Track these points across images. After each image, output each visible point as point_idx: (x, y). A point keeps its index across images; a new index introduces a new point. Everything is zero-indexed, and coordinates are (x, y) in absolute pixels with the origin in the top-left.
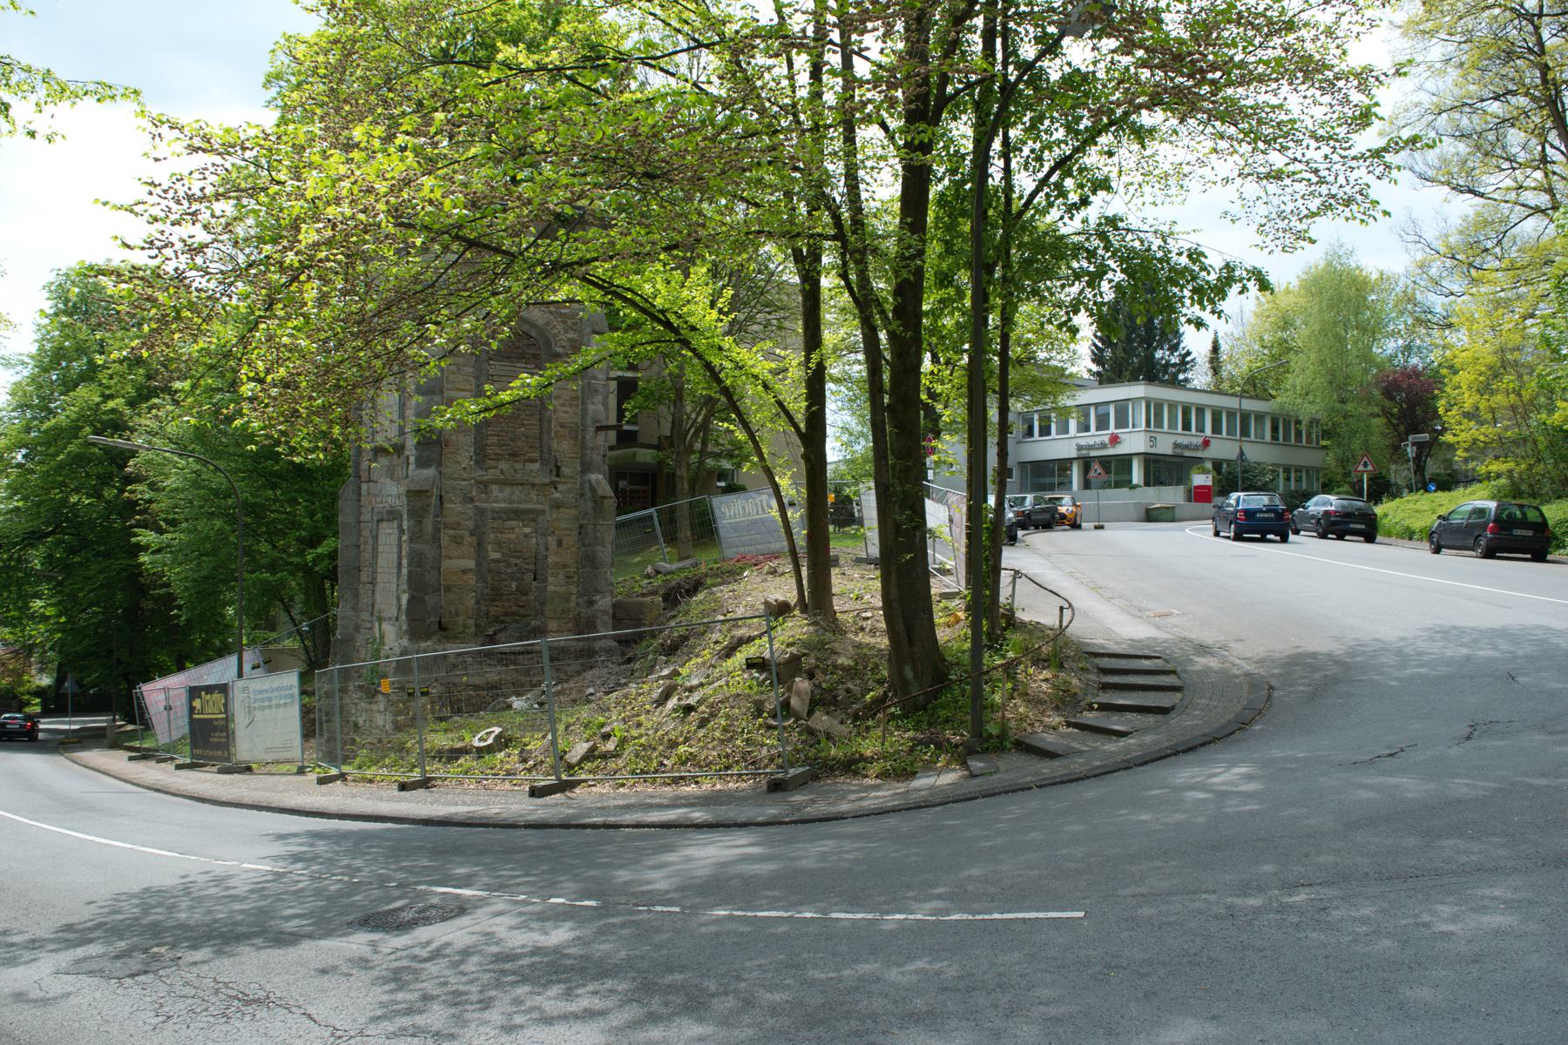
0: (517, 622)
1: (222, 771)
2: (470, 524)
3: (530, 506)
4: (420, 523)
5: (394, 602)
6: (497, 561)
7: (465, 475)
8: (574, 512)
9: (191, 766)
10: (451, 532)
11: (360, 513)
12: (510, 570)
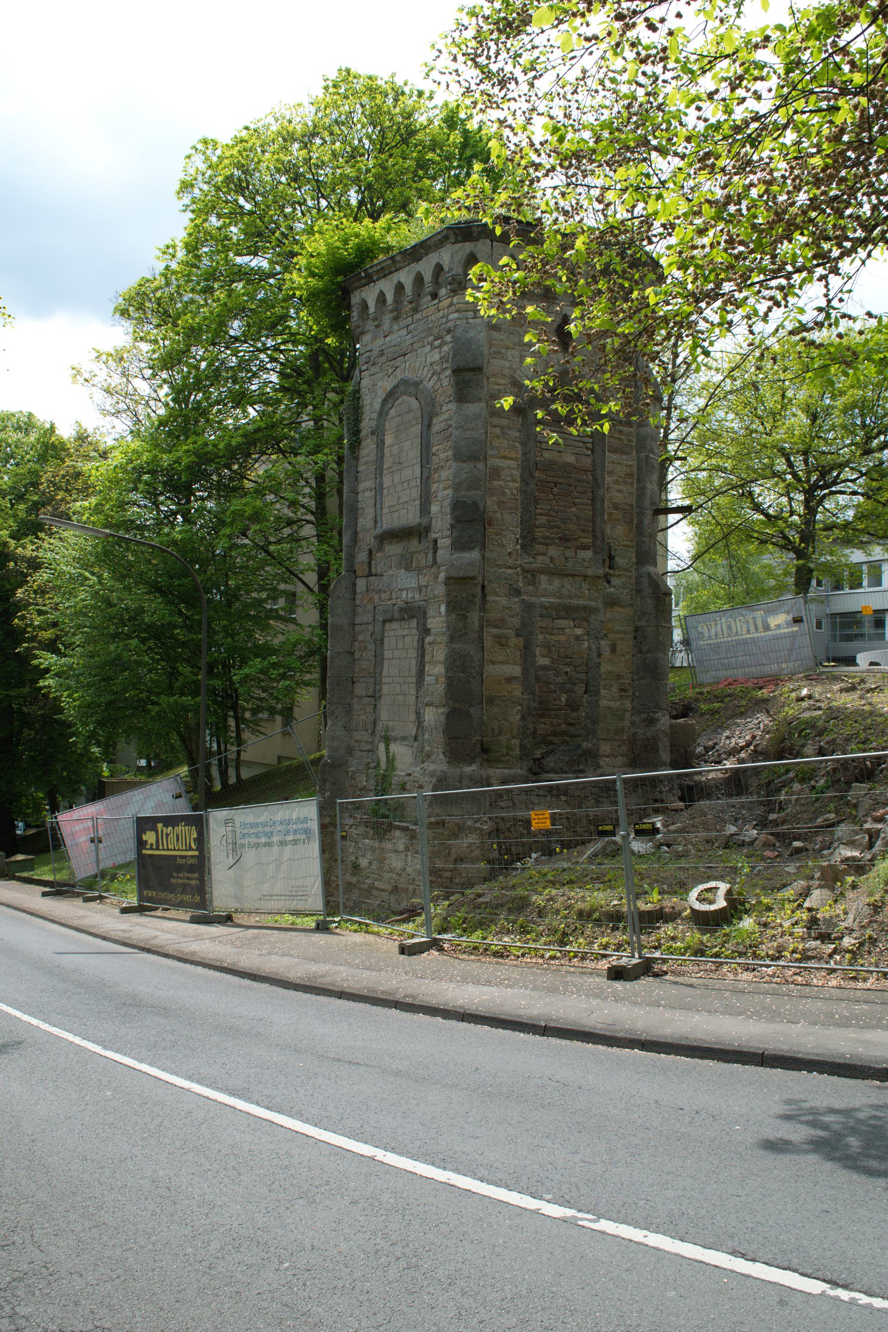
0: (565, 743)
1: (195, 920)
2: (516, 622)
3: (582, 602)
4: (464, 617)
5: (412, 717)
6: (544, 668)
7: (511, 562)
8: (629, 611)
9: (140, 910)
10: (495, 631)
11: (355, 614)
12: (560, 680)
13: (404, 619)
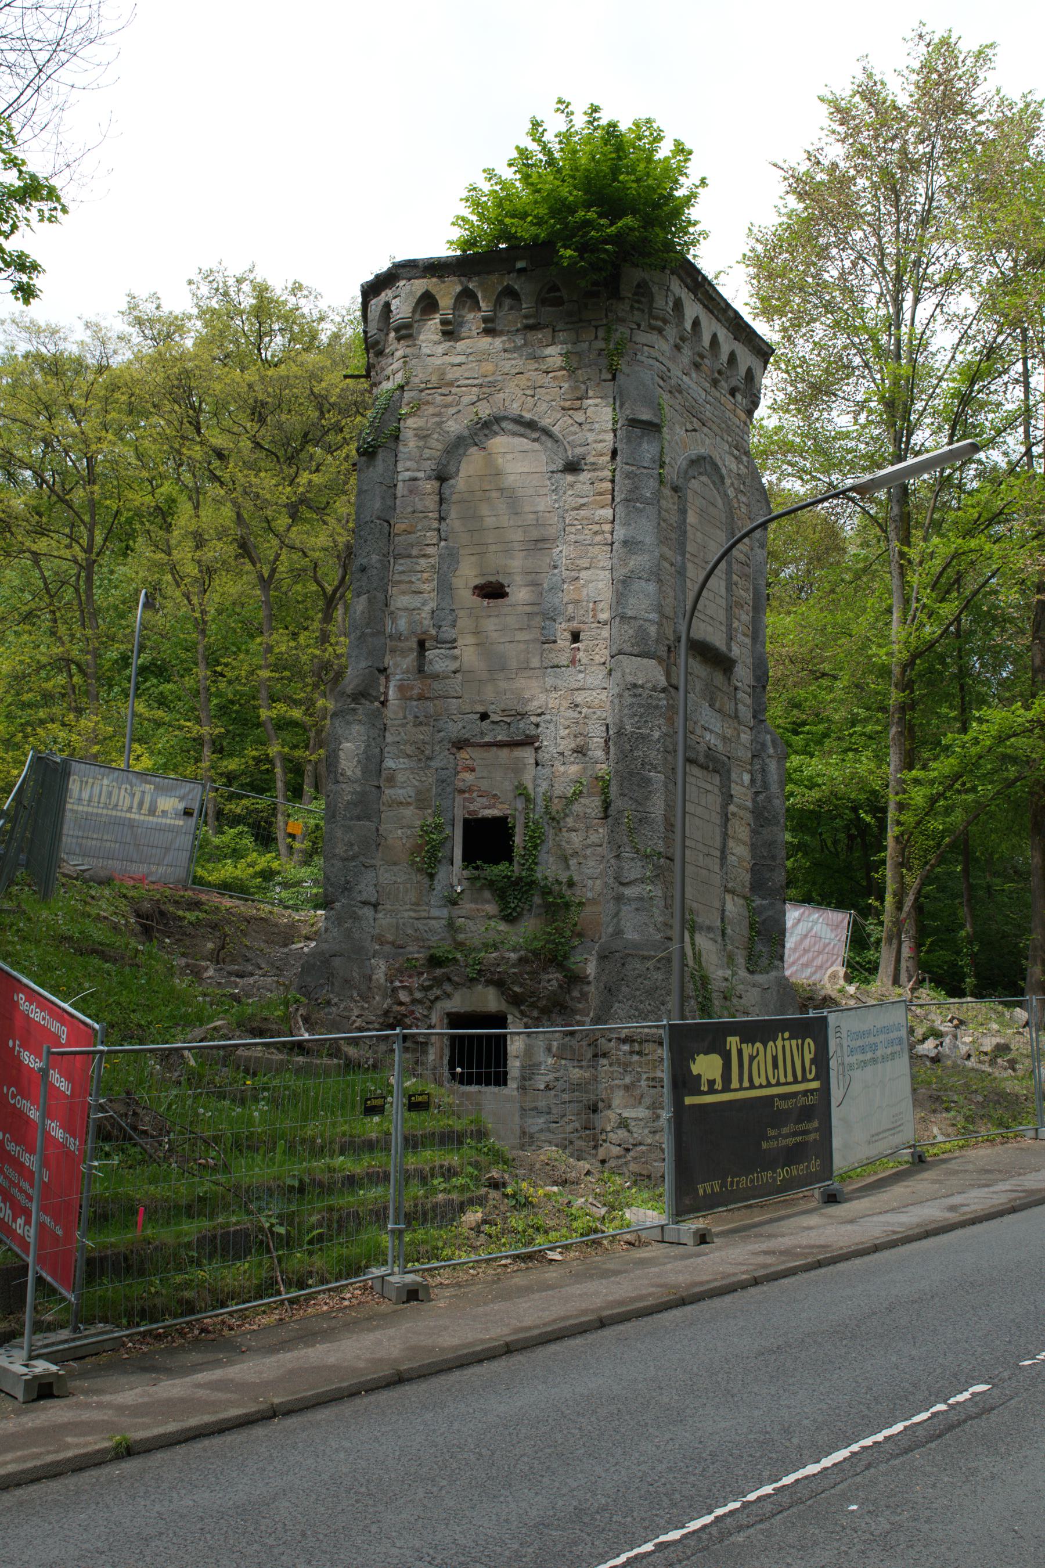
13: (707, 768)
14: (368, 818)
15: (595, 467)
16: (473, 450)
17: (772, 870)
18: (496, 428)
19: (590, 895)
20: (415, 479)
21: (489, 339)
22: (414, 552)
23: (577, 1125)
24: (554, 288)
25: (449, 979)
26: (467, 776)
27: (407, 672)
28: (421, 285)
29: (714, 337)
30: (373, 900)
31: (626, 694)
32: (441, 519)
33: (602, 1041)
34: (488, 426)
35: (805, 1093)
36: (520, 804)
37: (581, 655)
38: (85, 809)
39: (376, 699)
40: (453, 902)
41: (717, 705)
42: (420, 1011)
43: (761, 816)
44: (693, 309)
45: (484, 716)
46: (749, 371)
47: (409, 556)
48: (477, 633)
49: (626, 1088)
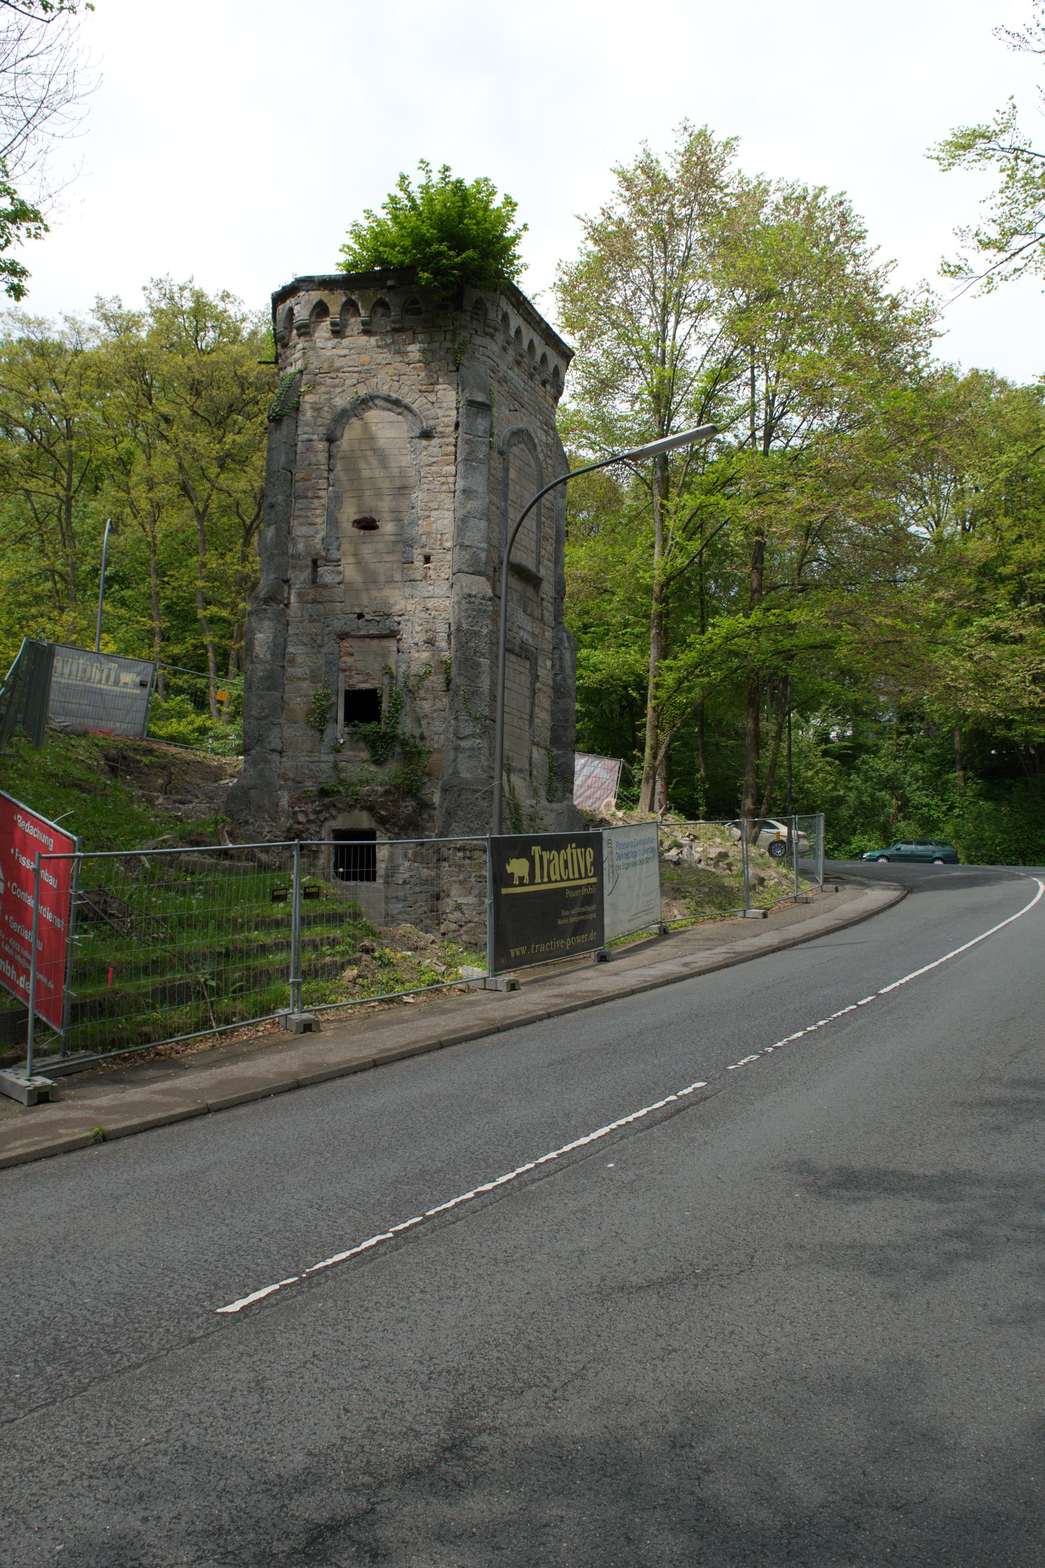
13: (520, 656)
14: (275, 689)
15: (443, 435)
16: (354, 420)
17: (565, 730)
18: (370, 404)
19: (436, 746)
20: (311, 440)
21: (366, 338)
22: (310, 494)
23: (426, 908)
24: (415, 302)
25: (334, 806)
26: (348, 659)
27: (304, 582)
28: (315, 296)
29: (531, 342)
30: (279, 748)
31: (463, 602)
32: (330, 470)
33: (444, 849)
34: (365, 403)
35: (587, 885)
36: (386, 680)
37: (431, 572)
38: (67, 681)
39: (282, 602)
40: (337, 750)
41: (529, 611)
42: (313, 828)
43: (559, 691)
44: (516, 321)
45: (360, 616)
46: (556, 368)
47: (306, 497)
48: (355, 555)
49: (461, 882)
